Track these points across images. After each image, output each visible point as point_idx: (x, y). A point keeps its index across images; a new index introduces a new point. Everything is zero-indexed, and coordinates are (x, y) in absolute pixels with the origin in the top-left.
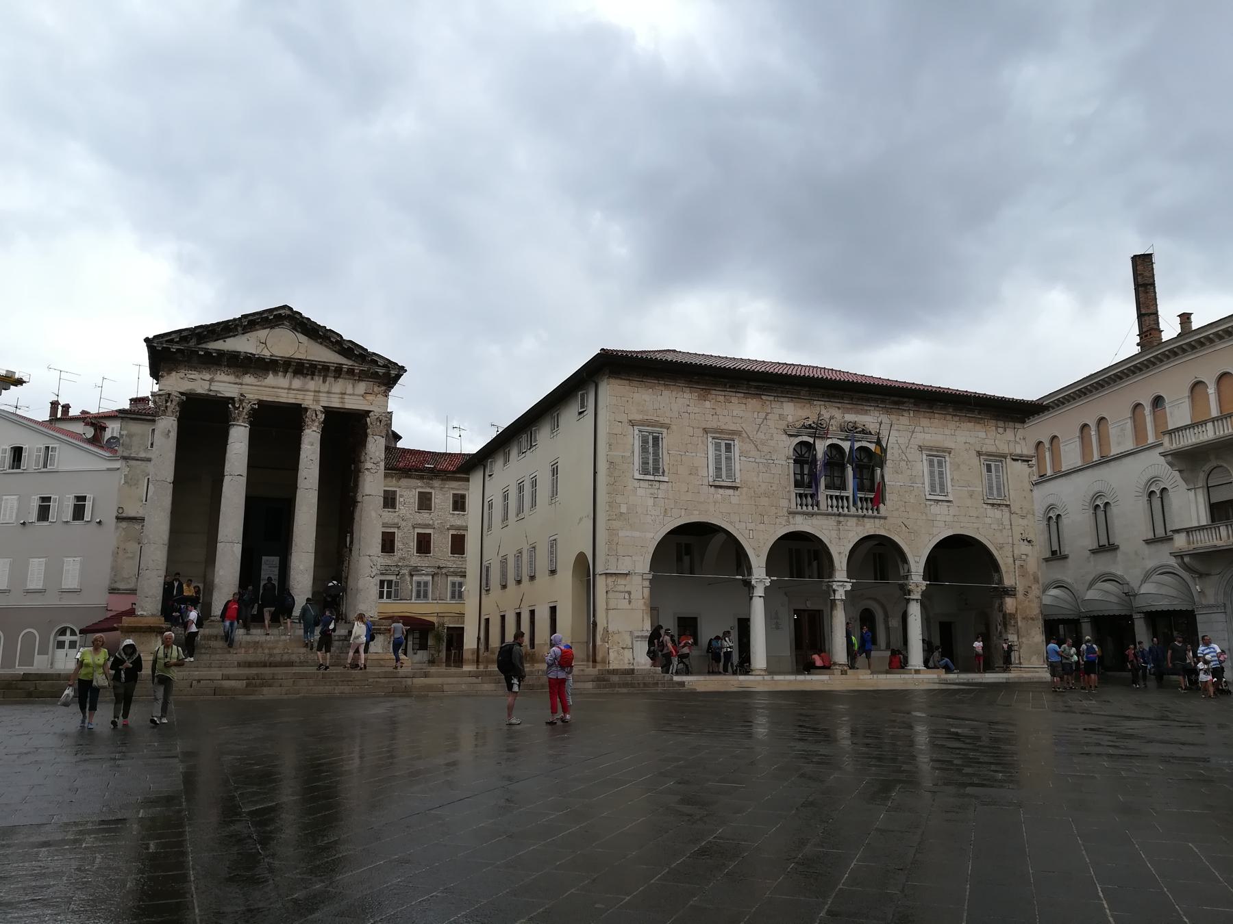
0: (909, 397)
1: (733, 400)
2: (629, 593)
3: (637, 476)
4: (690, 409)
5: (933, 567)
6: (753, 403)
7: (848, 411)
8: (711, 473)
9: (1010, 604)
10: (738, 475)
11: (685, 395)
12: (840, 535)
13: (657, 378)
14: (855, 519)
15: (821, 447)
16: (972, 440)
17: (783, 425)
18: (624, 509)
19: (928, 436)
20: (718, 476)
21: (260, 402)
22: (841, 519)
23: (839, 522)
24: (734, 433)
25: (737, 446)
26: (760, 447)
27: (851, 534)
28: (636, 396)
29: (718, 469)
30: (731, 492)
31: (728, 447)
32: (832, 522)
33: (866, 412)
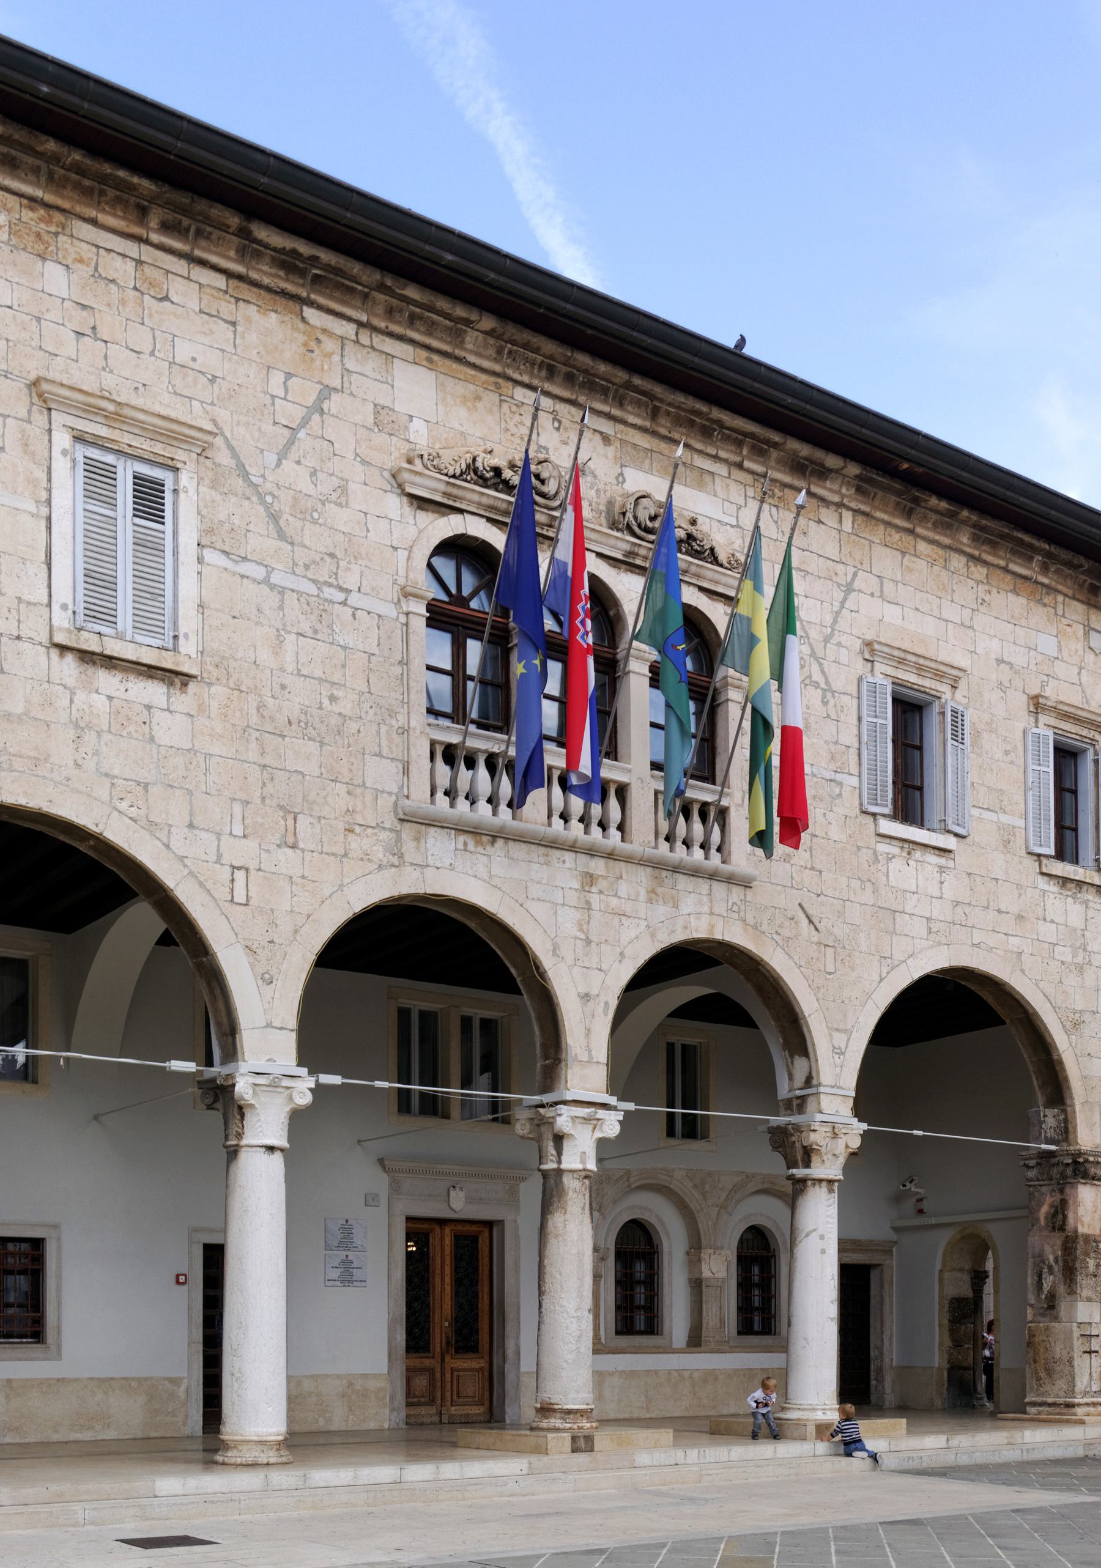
1: (178, 289)
6: (266, 327)
8: (63, 591)
10: (189, 622)
12: (586, 931)
14: (644, 875)
20: (100, 612)
22: (598, 866)
23: (589, 879)
24: (174, 433)
25: (188, 499)
26: (291, 524)
27: (630, 931)
29: (98, 580)
30: (154, 691)
31: (150, 499)
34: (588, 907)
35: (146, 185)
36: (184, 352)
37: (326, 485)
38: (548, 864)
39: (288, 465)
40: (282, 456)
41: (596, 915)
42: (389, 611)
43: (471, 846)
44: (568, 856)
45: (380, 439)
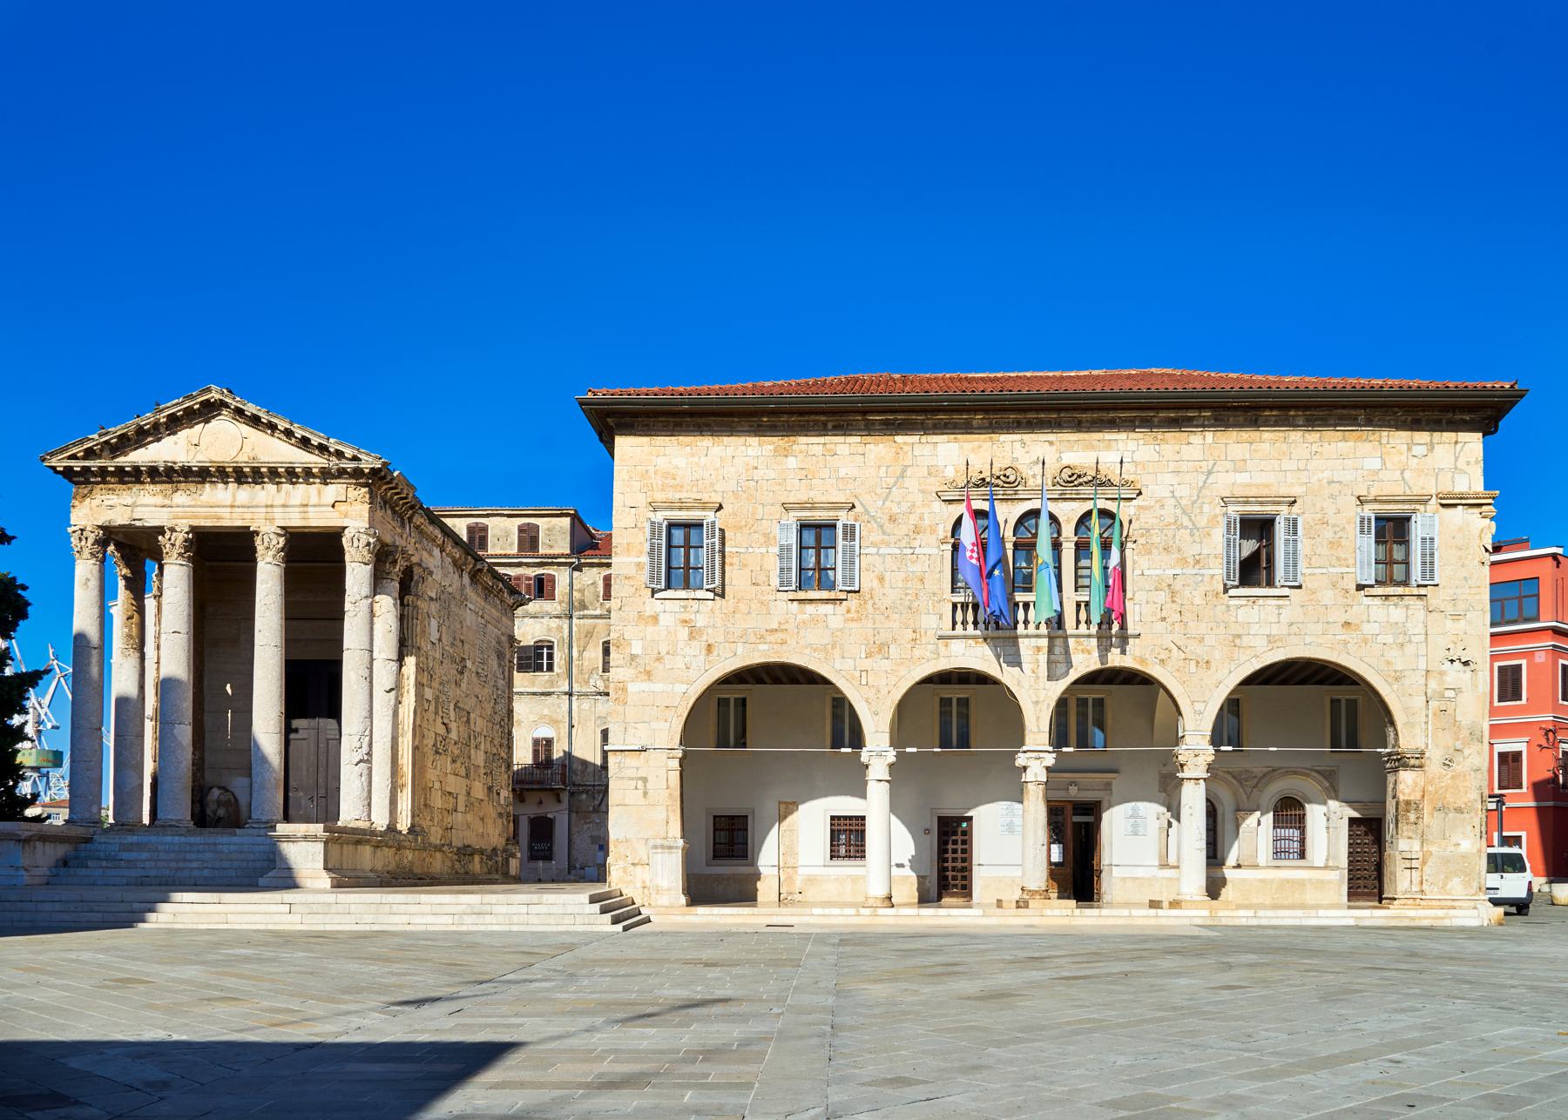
0: (1201, 407)
2: (645, 780)
4: (757, 475)
5: (1233, 722)
9: (1407, 783)
11: (750, 451)
15: (1008, 514)
16: (1347, 477)
17: (935, 485)
19: (1242, 478)
28: (661, 462)
30: (829, 608)
35: (823, 418)
36: (842, 473)
37: (905, 507)
39: (888, 504)
42: (935, 551)
45: (932, 480)
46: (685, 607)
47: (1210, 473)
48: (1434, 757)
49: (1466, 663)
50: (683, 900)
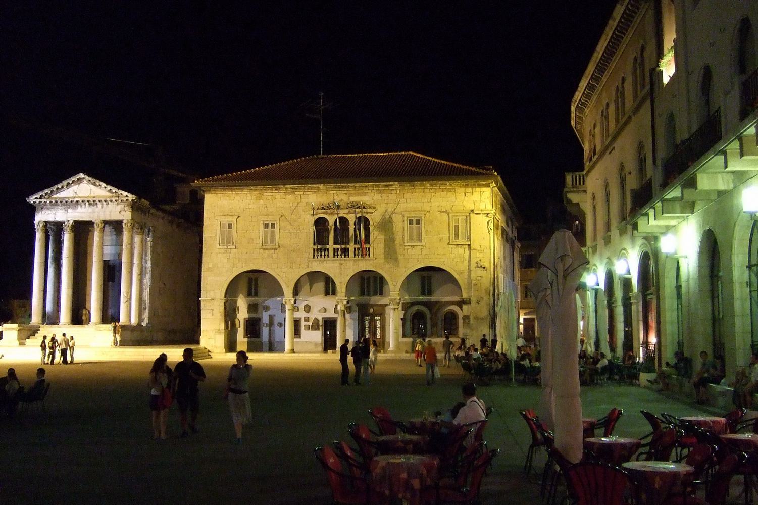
2: (213, 310)
3: (218, 246)
4: (251, 206)
6: (290, 197)
7: (351, 195)
13: (232, 191)
18: (210, 266)
19: (409, 205)
21: (75, 221)
22: (343, 262)
26: (293, 224)
32: (336, 264)
33: (365, 194)
34: (341, 268)
38: (333, 263)
40: (292, 214)
41: (343, 269)
43: (320, 262)
44: (337, 261)
46: (226, 251)
47: (399, 203)
48: (473, 300)
49: (484, 268)
50: (224, 351)
